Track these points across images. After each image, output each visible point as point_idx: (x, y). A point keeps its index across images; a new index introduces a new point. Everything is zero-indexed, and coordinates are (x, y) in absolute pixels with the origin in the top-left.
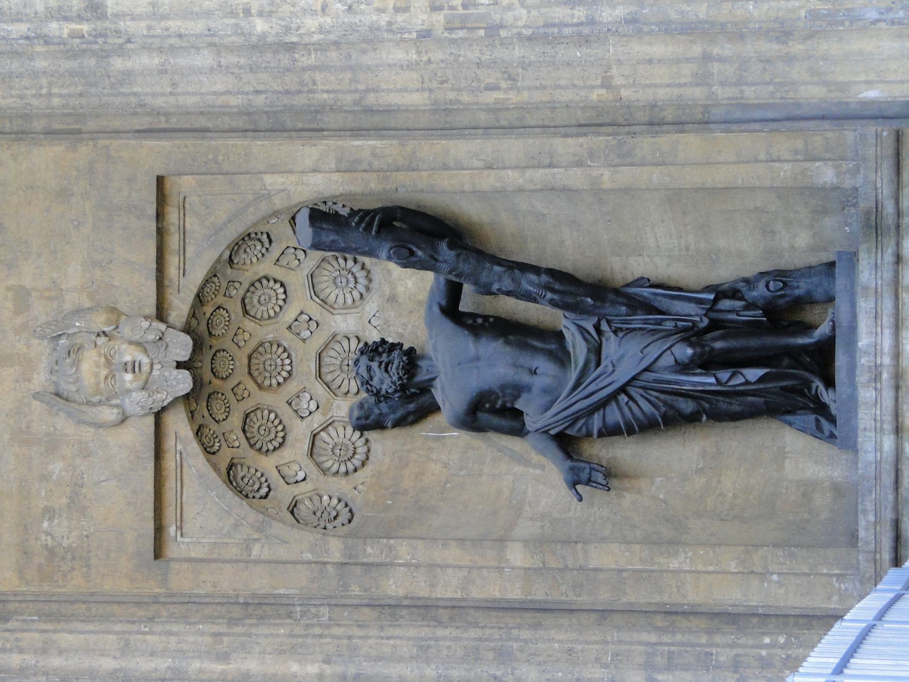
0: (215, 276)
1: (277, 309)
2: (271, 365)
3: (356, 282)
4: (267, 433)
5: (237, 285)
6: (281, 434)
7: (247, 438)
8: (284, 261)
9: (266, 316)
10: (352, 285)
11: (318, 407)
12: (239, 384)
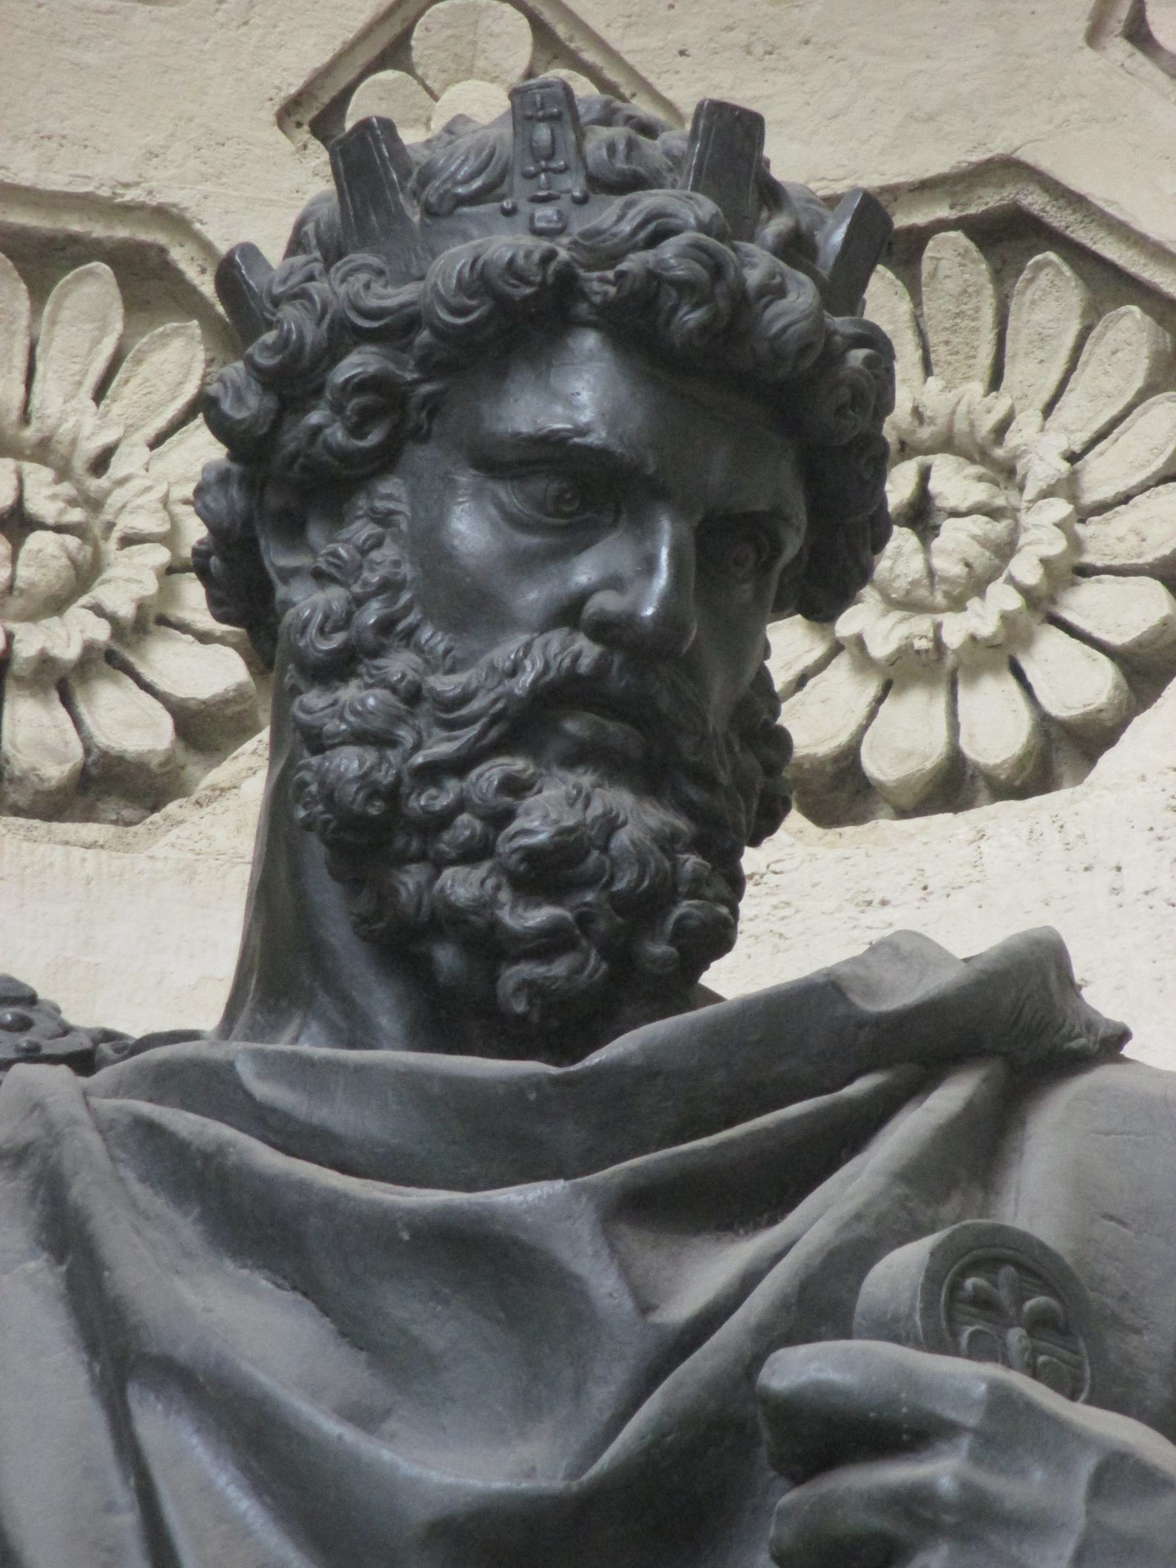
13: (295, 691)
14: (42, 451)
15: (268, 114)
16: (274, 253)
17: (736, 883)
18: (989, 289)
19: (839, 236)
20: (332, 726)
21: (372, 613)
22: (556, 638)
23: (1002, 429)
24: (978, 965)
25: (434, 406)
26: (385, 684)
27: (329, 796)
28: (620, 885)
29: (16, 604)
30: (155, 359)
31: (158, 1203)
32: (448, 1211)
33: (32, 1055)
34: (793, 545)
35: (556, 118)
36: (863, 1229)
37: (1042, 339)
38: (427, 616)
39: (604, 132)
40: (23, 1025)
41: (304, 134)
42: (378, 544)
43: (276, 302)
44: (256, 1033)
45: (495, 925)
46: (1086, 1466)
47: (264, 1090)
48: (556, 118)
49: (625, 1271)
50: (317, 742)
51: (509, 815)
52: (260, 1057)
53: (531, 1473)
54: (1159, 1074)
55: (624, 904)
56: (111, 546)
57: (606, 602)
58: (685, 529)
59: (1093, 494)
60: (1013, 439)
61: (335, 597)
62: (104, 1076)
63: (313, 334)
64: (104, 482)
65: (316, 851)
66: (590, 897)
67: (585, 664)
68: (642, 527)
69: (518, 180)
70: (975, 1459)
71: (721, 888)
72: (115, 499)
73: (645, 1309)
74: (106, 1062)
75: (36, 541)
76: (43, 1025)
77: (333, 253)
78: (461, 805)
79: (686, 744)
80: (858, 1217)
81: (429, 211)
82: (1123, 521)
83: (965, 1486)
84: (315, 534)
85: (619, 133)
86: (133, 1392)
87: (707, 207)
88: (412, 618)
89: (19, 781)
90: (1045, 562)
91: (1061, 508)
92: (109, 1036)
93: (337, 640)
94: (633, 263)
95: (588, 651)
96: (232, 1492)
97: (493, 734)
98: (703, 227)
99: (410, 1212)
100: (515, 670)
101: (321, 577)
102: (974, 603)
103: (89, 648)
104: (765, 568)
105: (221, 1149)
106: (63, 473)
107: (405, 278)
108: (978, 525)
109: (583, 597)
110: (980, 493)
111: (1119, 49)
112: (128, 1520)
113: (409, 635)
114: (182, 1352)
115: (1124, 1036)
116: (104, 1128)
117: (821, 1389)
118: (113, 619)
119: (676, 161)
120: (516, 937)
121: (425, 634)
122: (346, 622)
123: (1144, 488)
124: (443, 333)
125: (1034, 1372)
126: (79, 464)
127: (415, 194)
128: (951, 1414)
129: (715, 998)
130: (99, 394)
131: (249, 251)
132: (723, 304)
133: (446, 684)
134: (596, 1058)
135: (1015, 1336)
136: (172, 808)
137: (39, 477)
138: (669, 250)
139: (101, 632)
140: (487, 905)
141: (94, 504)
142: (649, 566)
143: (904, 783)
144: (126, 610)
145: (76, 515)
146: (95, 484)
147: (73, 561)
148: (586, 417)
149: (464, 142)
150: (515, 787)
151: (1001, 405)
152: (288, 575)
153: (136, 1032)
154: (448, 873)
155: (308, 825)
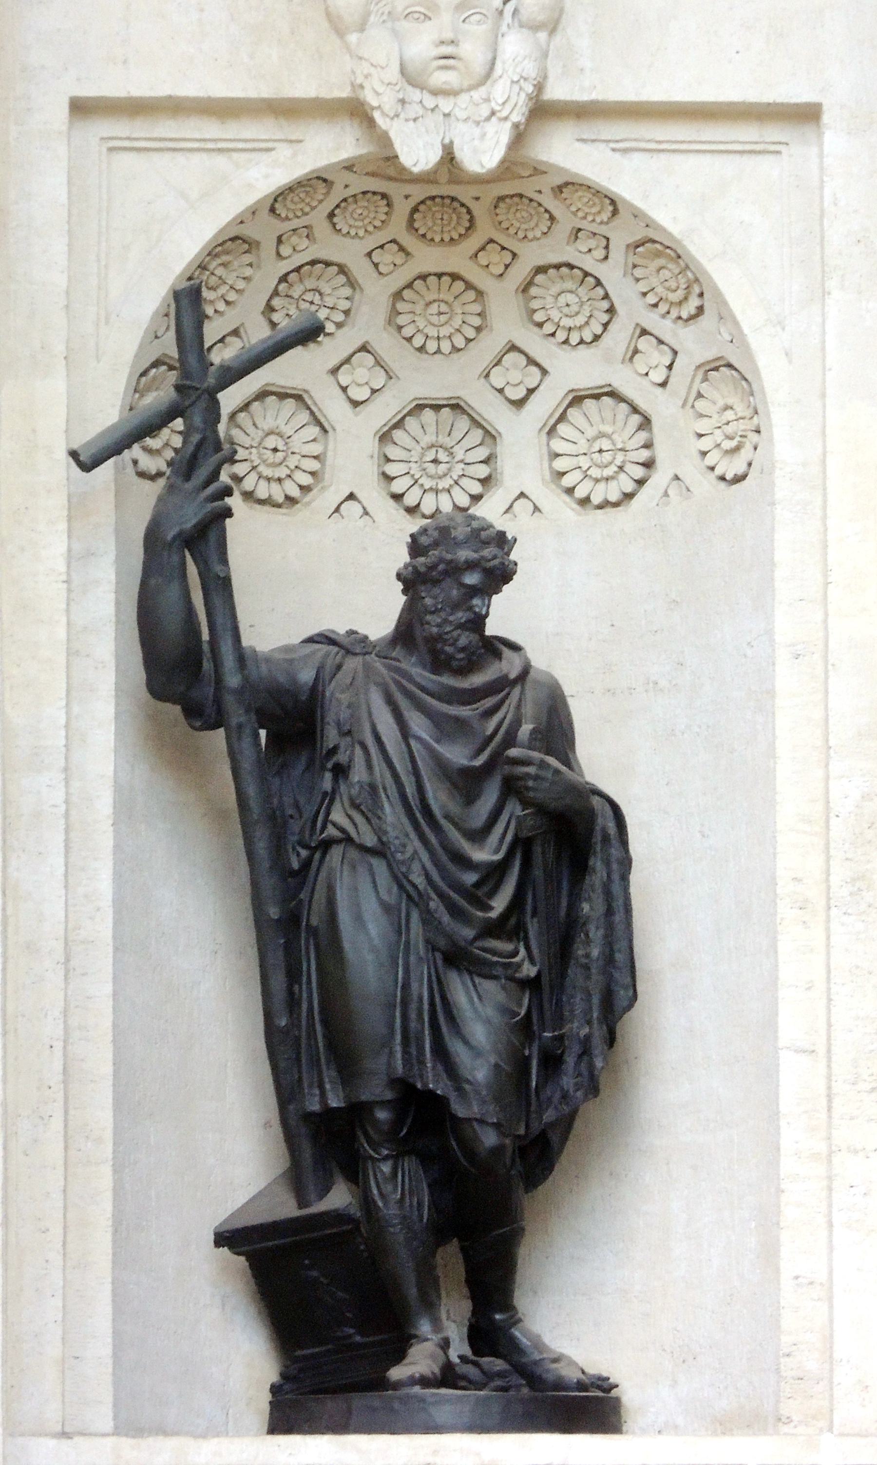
0: (615, 212)
3: (597, 481)
7: (298, 269)
9: (535, 304)
10: (595, 472)
11: (356, 404)
12: (408, 254)
82: (471, 467)
93: (433, 609)
94: (492, 563)
110: (447, 459)
111: (482, 380)
123: (477, 462)
128: (535, 762)
139: (288, 472)
150: (459, 635)
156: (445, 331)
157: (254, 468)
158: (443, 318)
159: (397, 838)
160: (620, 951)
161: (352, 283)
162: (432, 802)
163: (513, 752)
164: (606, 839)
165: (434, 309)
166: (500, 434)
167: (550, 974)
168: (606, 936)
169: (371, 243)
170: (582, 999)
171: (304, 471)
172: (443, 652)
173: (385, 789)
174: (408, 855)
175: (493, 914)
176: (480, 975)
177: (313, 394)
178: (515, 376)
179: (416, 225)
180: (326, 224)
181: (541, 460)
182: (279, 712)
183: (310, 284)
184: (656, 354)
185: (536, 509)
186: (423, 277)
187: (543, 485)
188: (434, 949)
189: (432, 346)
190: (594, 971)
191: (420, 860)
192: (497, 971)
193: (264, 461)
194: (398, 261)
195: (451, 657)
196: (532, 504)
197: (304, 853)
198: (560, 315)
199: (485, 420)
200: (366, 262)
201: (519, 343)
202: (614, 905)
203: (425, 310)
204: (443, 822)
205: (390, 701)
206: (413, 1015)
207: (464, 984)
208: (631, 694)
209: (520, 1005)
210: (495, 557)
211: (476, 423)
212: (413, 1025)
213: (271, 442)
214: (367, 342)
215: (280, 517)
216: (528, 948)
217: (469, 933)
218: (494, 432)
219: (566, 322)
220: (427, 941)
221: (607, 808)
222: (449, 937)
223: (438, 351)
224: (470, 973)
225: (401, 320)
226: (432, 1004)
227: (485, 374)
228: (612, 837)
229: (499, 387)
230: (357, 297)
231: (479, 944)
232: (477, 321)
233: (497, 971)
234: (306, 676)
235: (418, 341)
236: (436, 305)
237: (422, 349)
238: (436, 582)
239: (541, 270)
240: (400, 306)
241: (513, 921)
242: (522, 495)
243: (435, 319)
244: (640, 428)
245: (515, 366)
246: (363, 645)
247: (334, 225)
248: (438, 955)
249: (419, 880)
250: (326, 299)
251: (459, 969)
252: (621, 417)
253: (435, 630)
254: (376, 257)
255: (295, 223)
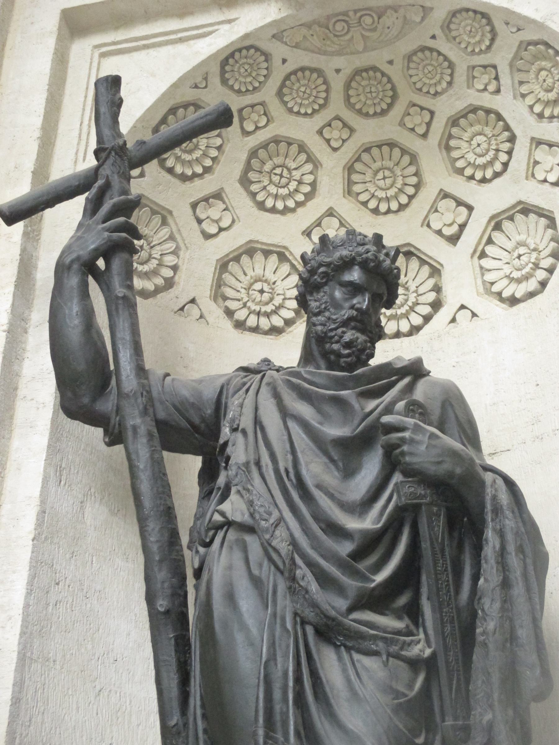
1: (469, 172)
2: (384, 178)
4: (276, 179)
5: (492, 87)
6: (280, 205)
8: (540, 154)
9: (455, 154)
10: (516, 275)
12: (352, 130)
13: (311, 317)
14: (266, 281)
15: (300, 233)
16: (309, 253)
17: (374, 348)
18: (405, 262)
19: (393, 253)
20: (317, 323)
21: (323, 306)
22: (350, 311)
23: (406, 283)
24: (411, 361)
25: (333, 276)
26: (324, 316)
27: (316, 333)
28: (359, 347)
29: (261, 303)
30: (282, 268)
31: (290, 391)
32: (334, 394)
33: (270, 369)
34: (385, 298)
35: (353, 235)
36: (395, 399)
37: (413, 270)
38: (331, 307)
39: (360, 237)
40: (269, 365)
41: (305, 236)
42: (324, 296)
43: (310, 260)
44: (303, 367)
45: (340, 352)
46: (428, 434)
47: (305, 376)
48: (353, 235)
49: (360, 404)
50: (315, 325)
51: (343, 337)
52: (305, 371)
53: (345, 433)
54: (436, 378)
55: (359, 350)
56: (275, 295)
57: (358, 306)
58: (370, 296)
59: (420, 293)
60: (408, 284)
61: (317, 304)
62: (280, 373)
63: (316, 265)
64: (275, 286)
65: (313, 341)
66: (354, 349)
67: (355, 315)
68: (363, 295)
69: (346, 244)
70: (412, 433)
71: (373, 348)
72: (276, 289)
73: (363, 409)
74: (281, 371)
75: (265, 294)
76: (272, 365)
77: (318, 253)
78: (336, 335)
79: (369, 328)
80: (394, 397)
81: (333, 247)
83: (410, 437)
84: (315, 294)
85: (362, 237)
86: (287, 419)
87: (375, 248)
88: (329, 307)
89: (261, 329)
90: (413, 302)
91: (415, 295)
92: (281, 367)
93: (318, 310)
94: (364, 256)
95: (355, 313)
96: (302, 434)
97: (341, 324)
98: (374, 251)
99: (328, 394)
100: (344, 315)
101: (316, 301)
102: (402, 308)
103: (272, 310)
104: (381, 301)
105: (300, 384)
106: (269, 284)
107: (329, 257)
108: (403, 297)
109: (354, 305)
111: (425, 228)
112: (286, 437)
113: (328, 310)
114: (295, 413)
115: (430, 372)
116: (282, 380)
117: (389, 422)
118: (275, 306)
119: (370, 241)
120: (343, 354)
121: (331, 310)
122: (319, 307)
123: (427, 292)
124: (335, 265)
125: (420, 421)
126: (271, 283)
127: (331, 245)
128: (408, 426)
129: (370, 365)
130: (274, 273)
131: (306, 253)
132: (377, 262)
133: (334, 317)
134: (355, 373)
135: (417, 415)
136: (283, 334)
137: (265, 285)
138: (369, 254)
139: (274, 308)
140: (339, 350)
141: (273, 289)
142: (364, 301)
143: (391, 334)
144: (277, 305)
145: (271, 291)
146: (273, 286)
147: (270, 298)
148: (356, 278)
149: (339, 238)
150: (344, 332)
151: (406, 279)
152: (310, 300)
153: (285, 366)
154: (333, 345)
155: (313, 337)
156: (391, 193)
157: (245, 305)
158: (388, 181)
159: (262, 506)
160: (521, 627)
161: (310, 159)
162: (304, 472)
163: (386, 419)
164: (497, 510)
165: (380, 175)
166: (442, 265)
167: (446, 655)
168: (503, 609)
169: (319, 120)
170: (483, 682)
171: (289, 309)
172: (333, 352)
173: (258, 464)
174: (272, 521)
175: (373, 585)
176: (359, 651)
177: (291, 250)
178: (448, 217)
179: (353, 100)
180: (276, 101)
181: (475, 279)
182: (184, 424)
183: (278, 160)
184: (550, 158)
185: (474, 315)
186: (367, 150)
187: (478, 295)
188: (304, 623)
189: (383, 207)
190: (491, 646)
191: (288, 529)
192: (377, 646)
193: (253, 301)
194: (345, 137)
195: (339, 355)
196: (470, 311)
197: (202, 550)
198: (475, 157)
199: (431, 258)
200: (317, 137)
201: (448, 190)
202: (512, 576)
203: (374, 178)
204: (317, 494)
205: (277, 396)
206: (277, 695)
207: (340, 659)
208: (555, 434)
209: (410, 686)
210: (368, 252)
211: (423, 262)
212: (278, 708)
213: (258, 286)
214: (331, 208)
215: (267, 340)
216: (425, 632)
217: (342, 604)
218: (438, 266)
219: (481, 161)
220: (296, 614)
221: (500, 482)
222: (314, 605)
223: (389, 211)
224: (348, 649)
225: (357, 188)
226: (298, 680)
227: (426, 222)
228: (505, 508)
229: (437, 229)
230: (320, 172)
231: (356, 615)
232: (414, 180)
233: (377, 646)
234: (210, 393)
235: (372, 204)
236: (381, 172)
237: (376, 211)
238: (317, 288)
239: (454, 122)
240: (355, 177)
241: (403, 600)
242: (463, 307)
243: (381, 183)
244: (548, 227)
245: (448, 210)
246: (267, 363)
247: (285, 103)
248: (310, 630)
249: (284, 547)
250: (294, 173)
251: (337, 647)
252: (532, 226)
253: (319, 328)
254: (327, 133)
255: (248, 99)
